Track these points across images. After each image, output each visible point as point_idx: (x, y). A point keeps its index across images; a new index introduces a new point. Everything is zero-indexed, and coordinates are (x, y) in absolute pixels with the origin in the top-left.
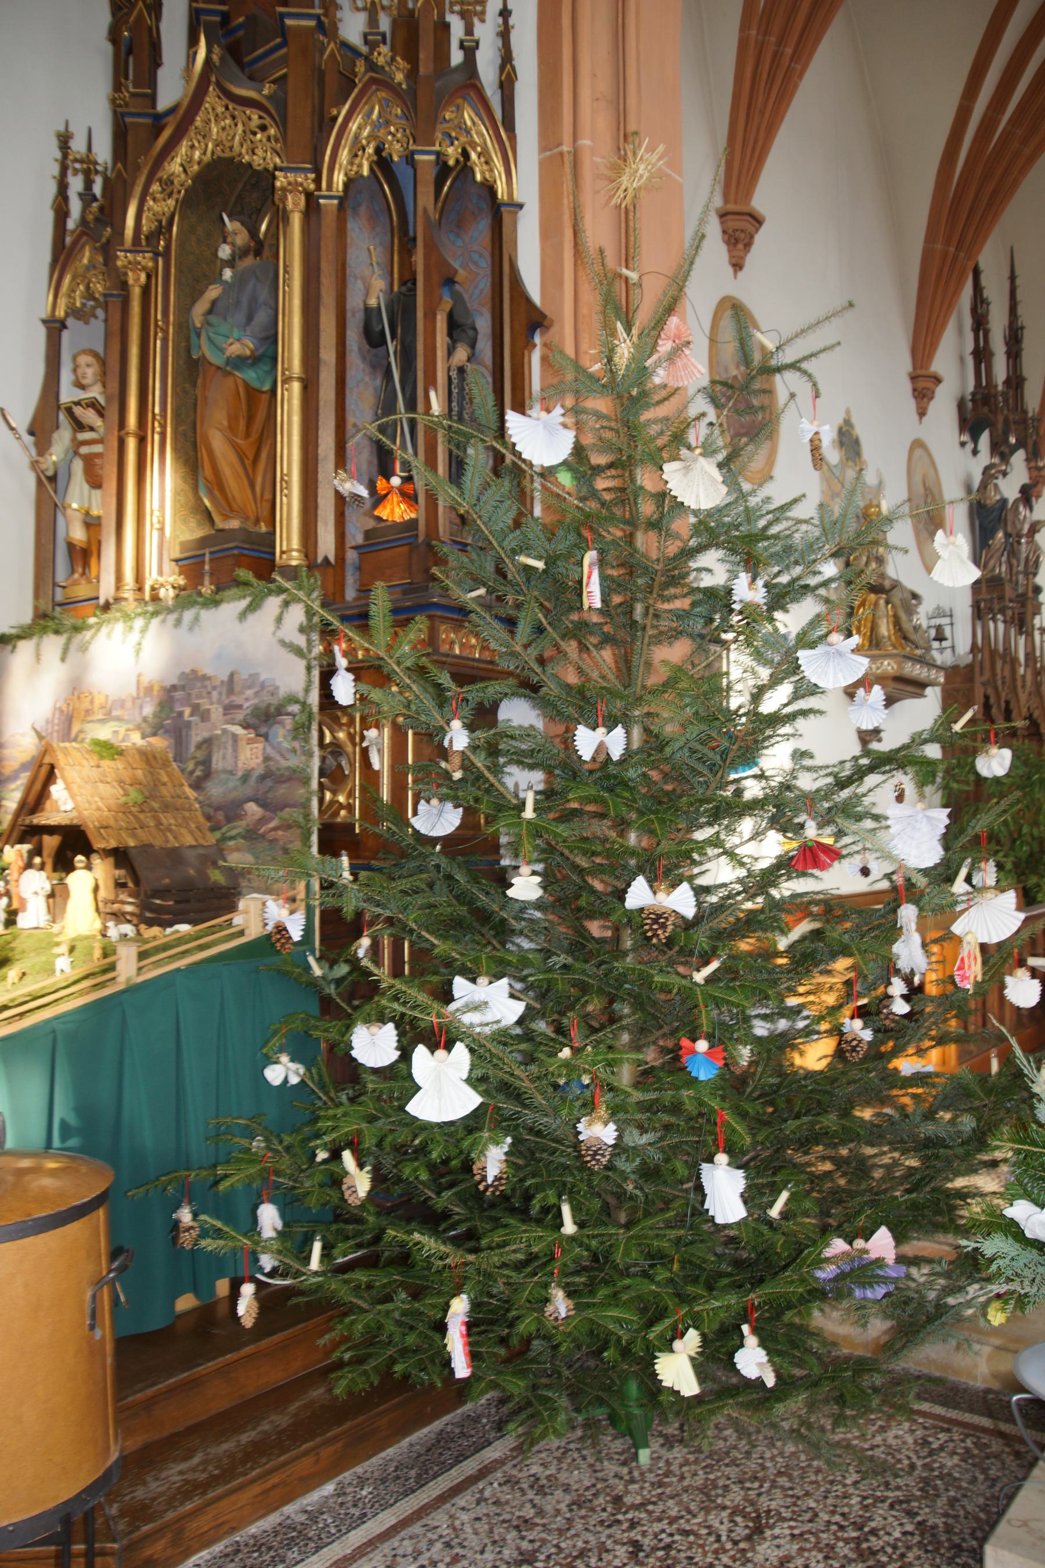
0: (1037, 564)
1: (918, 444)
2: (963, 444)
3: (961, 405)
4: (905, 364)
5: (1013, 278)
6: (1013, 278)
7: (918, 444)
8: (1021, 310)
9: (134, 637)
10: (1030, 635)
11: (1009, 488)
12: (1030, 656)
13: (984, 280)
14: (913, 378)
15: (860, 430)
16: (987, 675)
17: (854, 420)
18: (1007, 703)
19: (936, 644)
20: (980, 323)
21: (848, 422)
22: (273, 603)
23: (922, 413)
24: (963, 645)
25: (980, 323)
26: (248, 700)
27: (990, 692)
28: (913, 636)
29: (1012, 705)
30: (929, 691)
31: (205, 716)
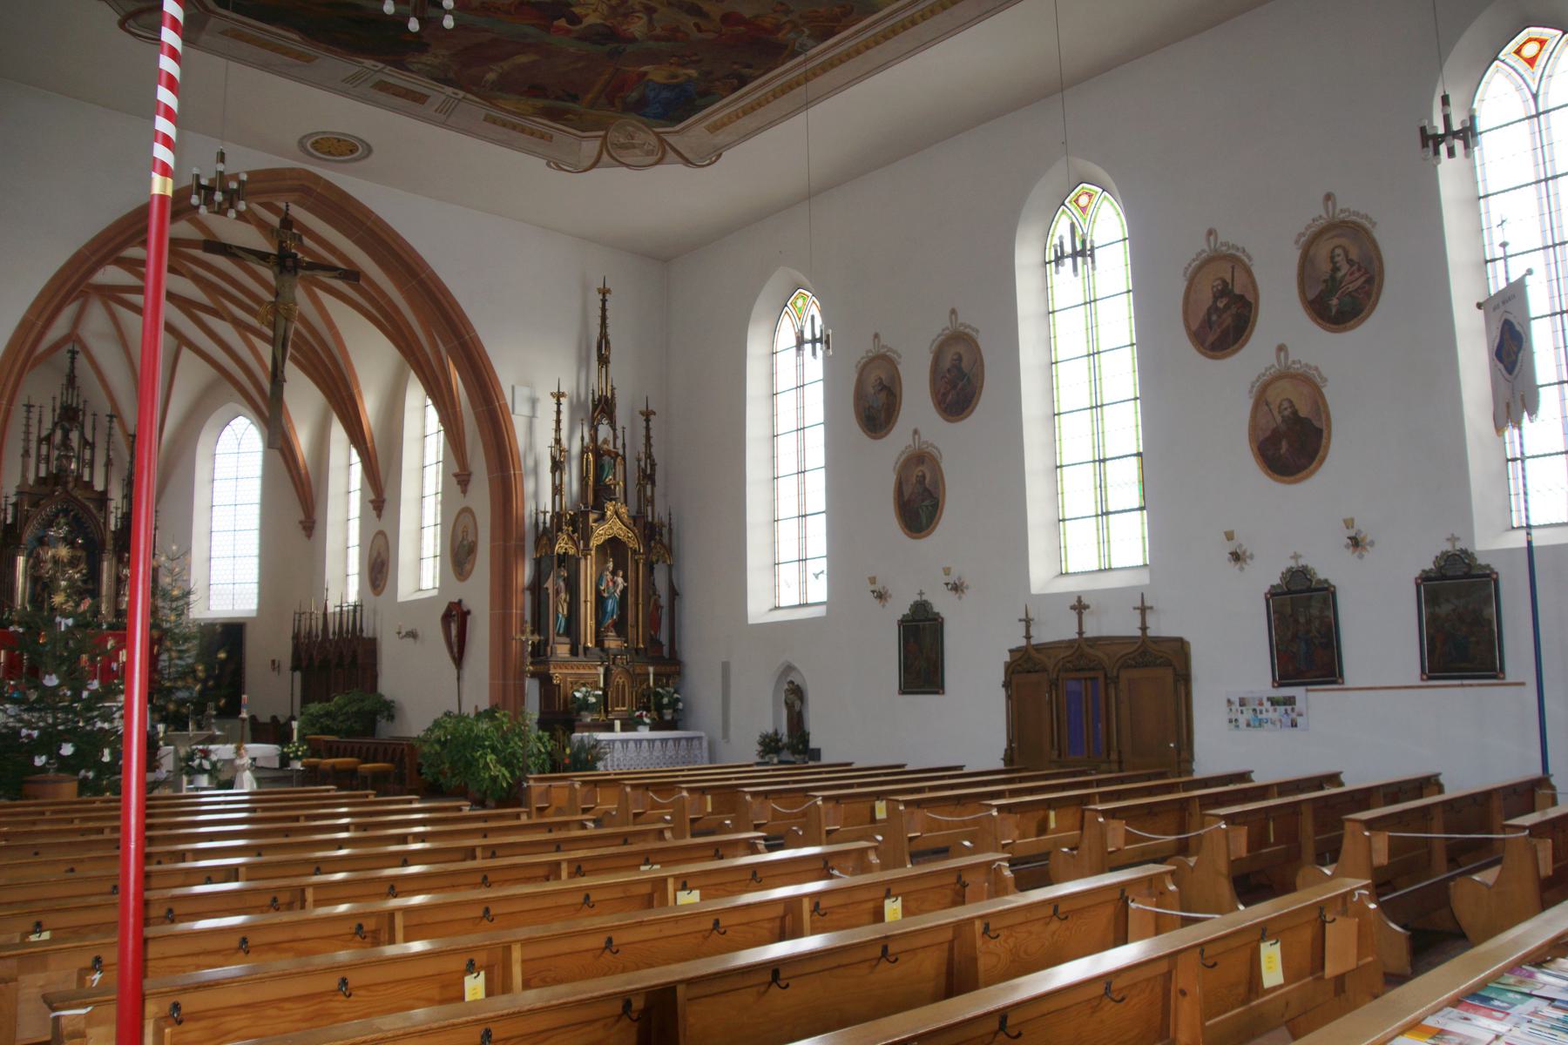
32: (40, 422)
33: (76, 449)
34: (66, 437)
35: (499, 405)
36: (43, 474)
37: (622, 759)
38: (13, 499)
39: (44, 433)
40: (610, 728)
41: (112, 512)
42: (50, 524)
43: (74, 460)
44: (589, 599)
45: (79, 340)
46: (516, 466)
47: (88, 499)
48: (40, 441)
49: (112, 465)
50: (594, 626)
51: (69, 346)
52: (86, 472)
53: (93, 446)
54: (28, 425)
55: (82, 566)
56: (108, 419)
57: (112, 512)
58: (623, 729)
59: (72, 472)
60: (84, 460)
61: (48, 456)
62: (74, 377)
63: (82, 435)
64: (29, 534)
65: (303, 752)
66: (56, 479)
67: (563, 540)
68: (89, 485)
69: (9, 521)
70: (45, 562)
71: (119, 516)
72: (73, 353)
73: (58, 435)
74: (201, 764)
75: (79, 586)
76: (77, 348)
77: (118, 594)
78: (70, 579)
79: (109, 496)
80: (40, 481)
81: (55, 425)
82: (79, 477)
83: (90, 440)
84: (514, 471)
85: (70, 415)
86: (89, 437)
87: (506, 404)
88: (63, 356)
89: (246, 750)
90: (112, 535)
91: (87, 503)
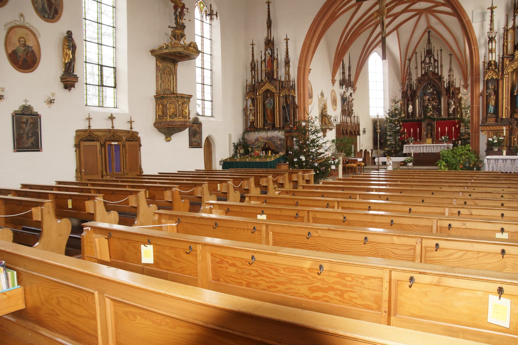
0: (353, 106)
1: (333, 90)
2: (340, 88)
3: (340, 82)
4: (331, 78)
5: (349, 58)
6: (349, 58)
7: (333, 90)
8: (351, 63)
9: (266, 133)
10: (351, 118)
11: (348, 94)
12: (351, 122)
13: (344, 61)
14: (332, 80)
15: (324, 92)
16: (343, 126)
17: (323, 91)
18: (346, 130)
19: (335, 121)
20: (343, 68)
21: (322, 92)
22: (281, 132)
23: (333, 85)
24: (339, 122)
25: (343, 68)
26: (279, 138)
27: (343, 128)
28: (331, 122)
29: (347, 130)
30: (333, 130)
31: (274, 139)
32: (421, 57)
33: (433, 63)
34: (430, 59)
35: (466, 21)
36: (423, 73)
37: (502, 167)
38: (415, 83)
39: (422, 61)
40: (501, 154)
41: (444, 82)
42: (425, 88)
43: (431, 67)
44: (504, 97)
45: (431, 27)
46: (475, 45)
47: (436, 79)
48: (422, 63)
49: (443, 66)
50: (509, 108)
51: (428, 31)
52: (436, 70)
53: (438, 61)
54: (416, 59)
55: (436, 100)
56: (440, 51)
57: (444, 82)
58: (507, 154)
59: (431, 71)
60: (435, 66)
61: (424, 67)
62: (430, 40)
63: (434, 58)
64: (418, 94)
65: (410, 160)
66: (426, 74)
67: (491, 73)
68: (438, 73)
69: (415, 89)
70: (426, 100)
71: (448, 82)
72: (429, 32)
73: (427, 60)
74: (331, 162)
75: (436, 107)
76: (431, 30)
77: (448, 109)
78: (433, 106)
79: (442, 77)
80: (422, 75)
81: (425, 57)
82: (434, 73)
83: (437, 59)
84: (474, 47)
85: (429, 53)
86: (436, 58)
87: (469, 20)
88: (427, 34)
89: (390, 159)
90: (445, 89)
91: (435, 80)
